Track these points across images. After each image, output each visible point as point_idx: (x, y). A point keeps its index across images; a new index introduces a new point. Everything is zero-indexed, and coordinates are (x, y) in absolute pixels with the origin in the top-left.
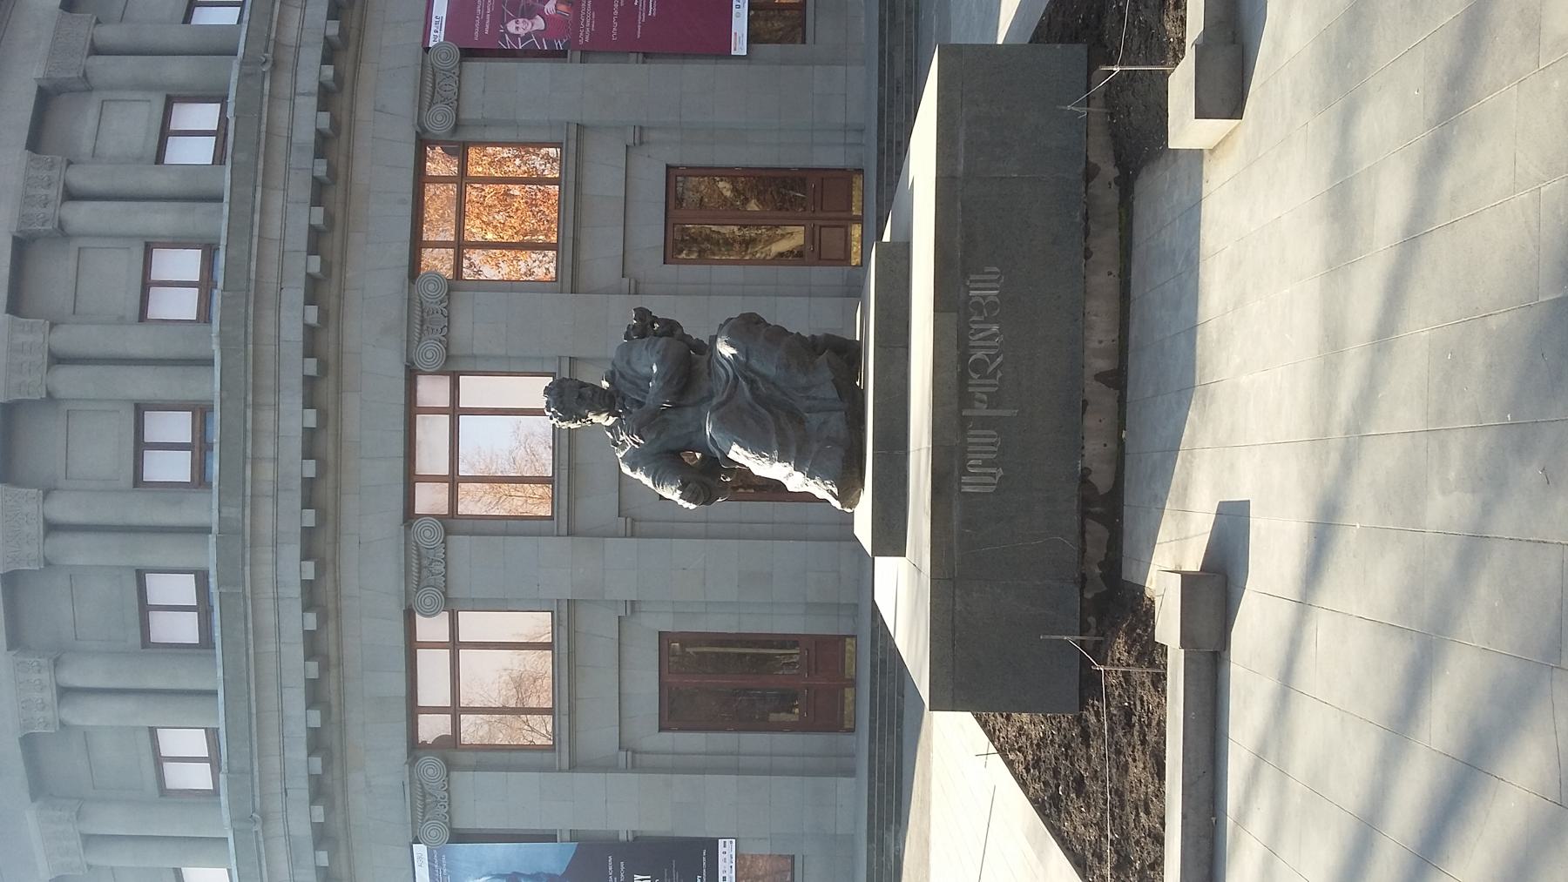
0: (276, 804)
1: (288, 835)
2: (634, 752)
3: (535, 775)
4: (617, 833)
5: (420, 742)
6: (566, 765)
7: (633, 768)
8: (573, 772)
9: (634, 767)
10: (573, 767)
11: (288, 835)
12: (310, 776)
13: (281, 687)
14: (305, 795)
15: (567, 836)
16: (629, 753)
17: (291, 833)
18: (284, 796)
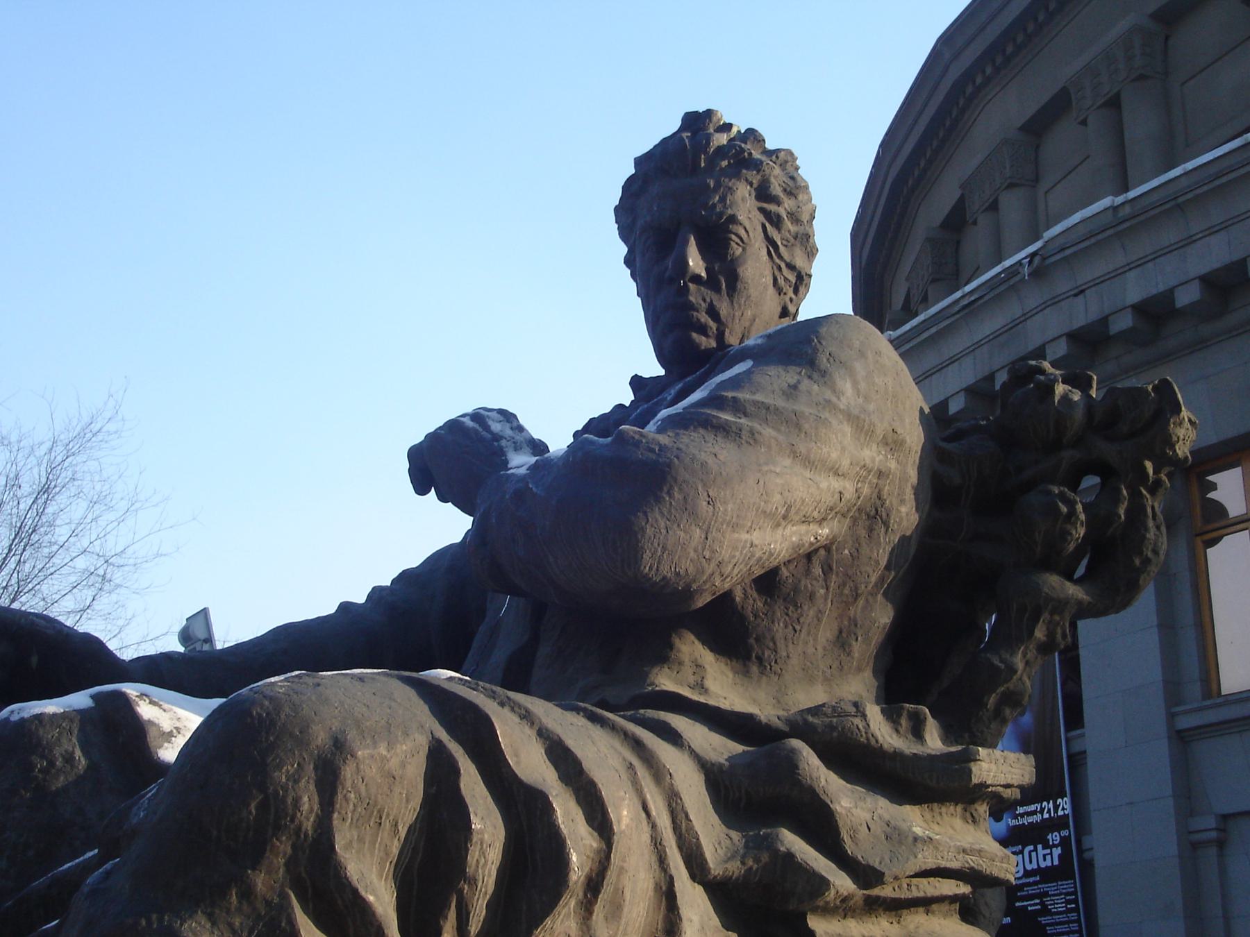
0: (1062, 284)
1: (1026, 317)
2: (1221, 844)
3: (1152, 671)
4: (1090, 832)
5: (1210, 478)
6: (1185, 722)
7: (1191, 848)
8: (1169, 738)
9: (1195, 846)
10: (1182, 739)
11: (1026, 317)
12: (1104, 321)
13: (1224, 227)
14: (1079, 321)
15: (1077, 747)
16: (1214, 834)
17: (1029, 322)
18: (1072, 293)
